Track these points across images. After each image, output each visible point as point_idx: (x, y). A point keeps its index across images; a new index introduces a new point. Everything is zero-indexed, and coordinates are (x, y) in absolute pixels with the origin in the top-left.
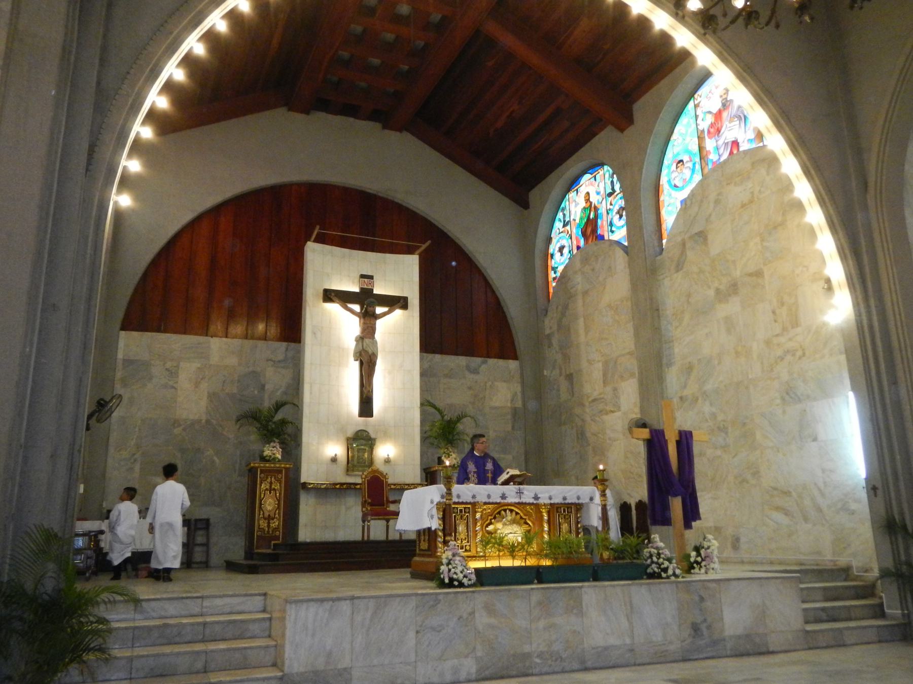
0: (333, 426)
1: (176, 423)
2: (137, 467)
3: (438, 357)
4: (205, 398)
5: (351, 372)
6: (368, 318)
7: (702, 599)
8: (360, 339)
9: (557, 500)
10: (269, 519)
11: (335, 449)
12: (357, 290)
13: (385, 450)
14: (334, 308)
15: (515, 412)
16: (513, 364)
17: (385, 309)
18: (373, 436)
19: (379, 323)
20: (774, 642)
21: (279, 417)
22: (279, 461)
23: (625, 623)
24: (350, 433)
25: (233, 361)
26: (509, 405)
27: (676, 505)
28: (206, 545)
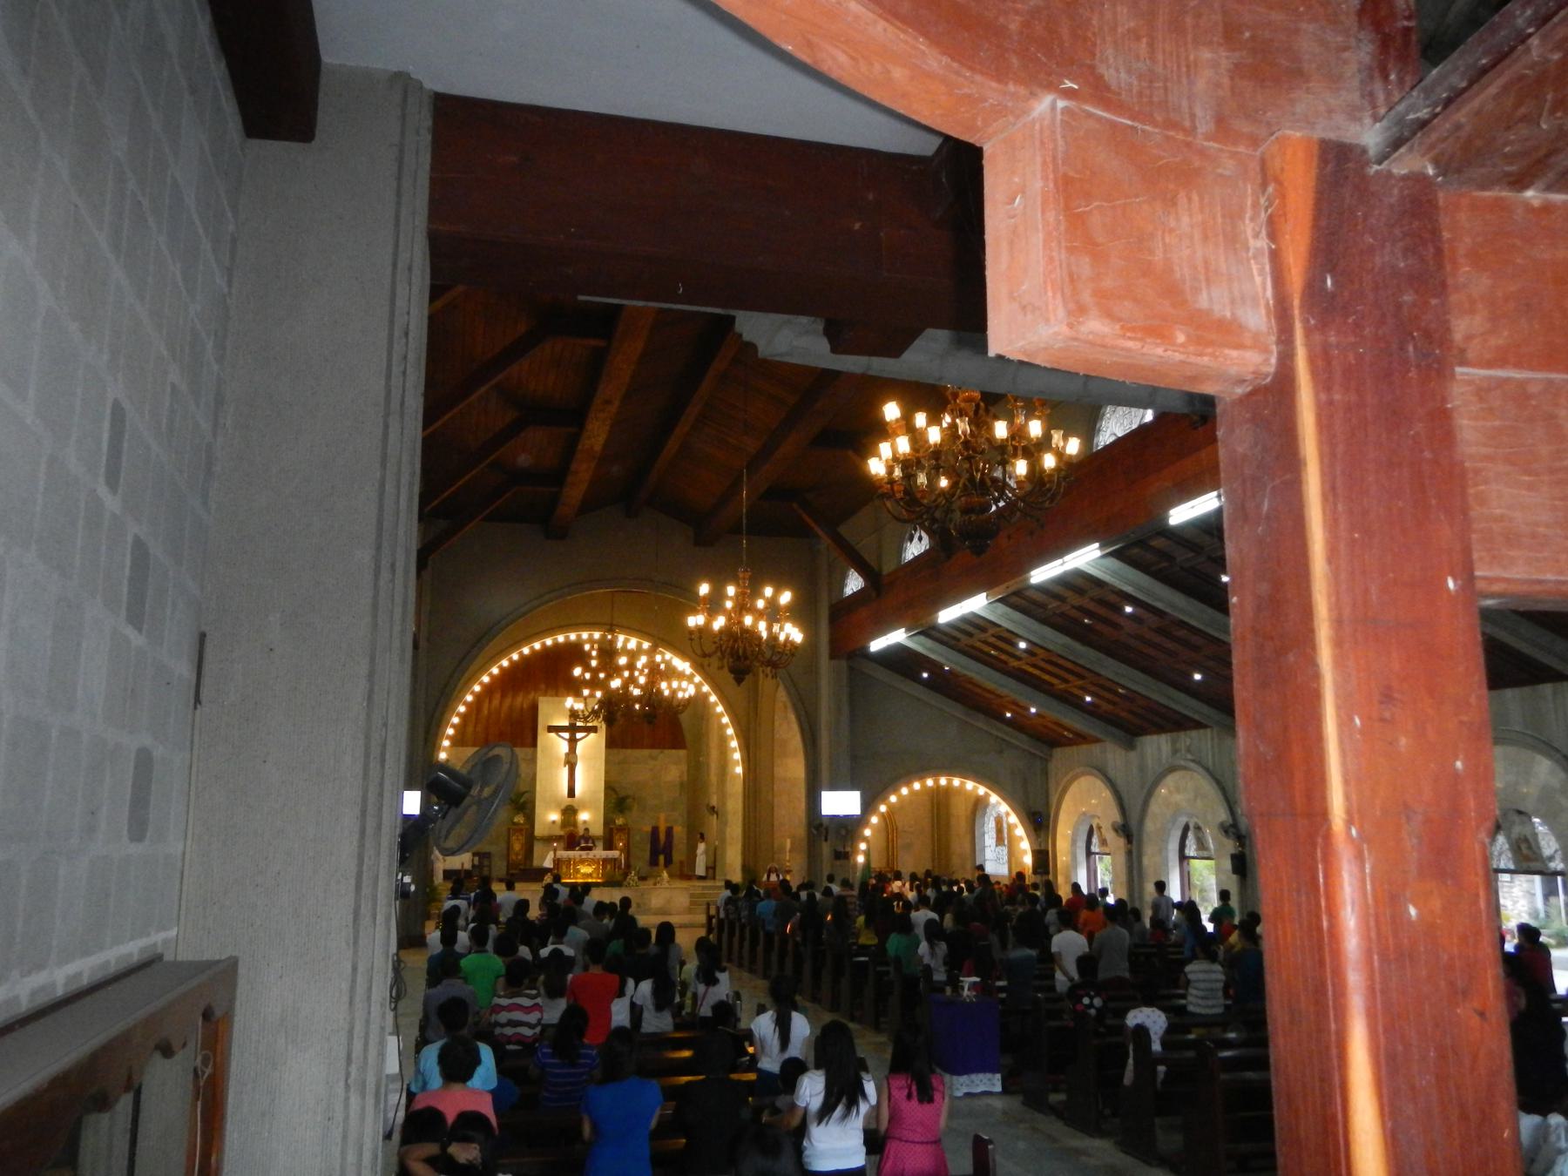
3: (629, 751)
5: (565, 771)
6: (573, 742)
8: (567, 755)
9: (604, 857)
10: (517, 854)
11: (554, 816)
12: (565, 723)
13: (584, 816)
14: (553, 735)
15: (682, 784)
16: (682, 753)
17: (583, 734)
18: (576, 807)
19: (578, 743)
22: (522, 824)
24: (563, 807)
26: (678, 779)
27: (662, 858)
28: (490, 866)
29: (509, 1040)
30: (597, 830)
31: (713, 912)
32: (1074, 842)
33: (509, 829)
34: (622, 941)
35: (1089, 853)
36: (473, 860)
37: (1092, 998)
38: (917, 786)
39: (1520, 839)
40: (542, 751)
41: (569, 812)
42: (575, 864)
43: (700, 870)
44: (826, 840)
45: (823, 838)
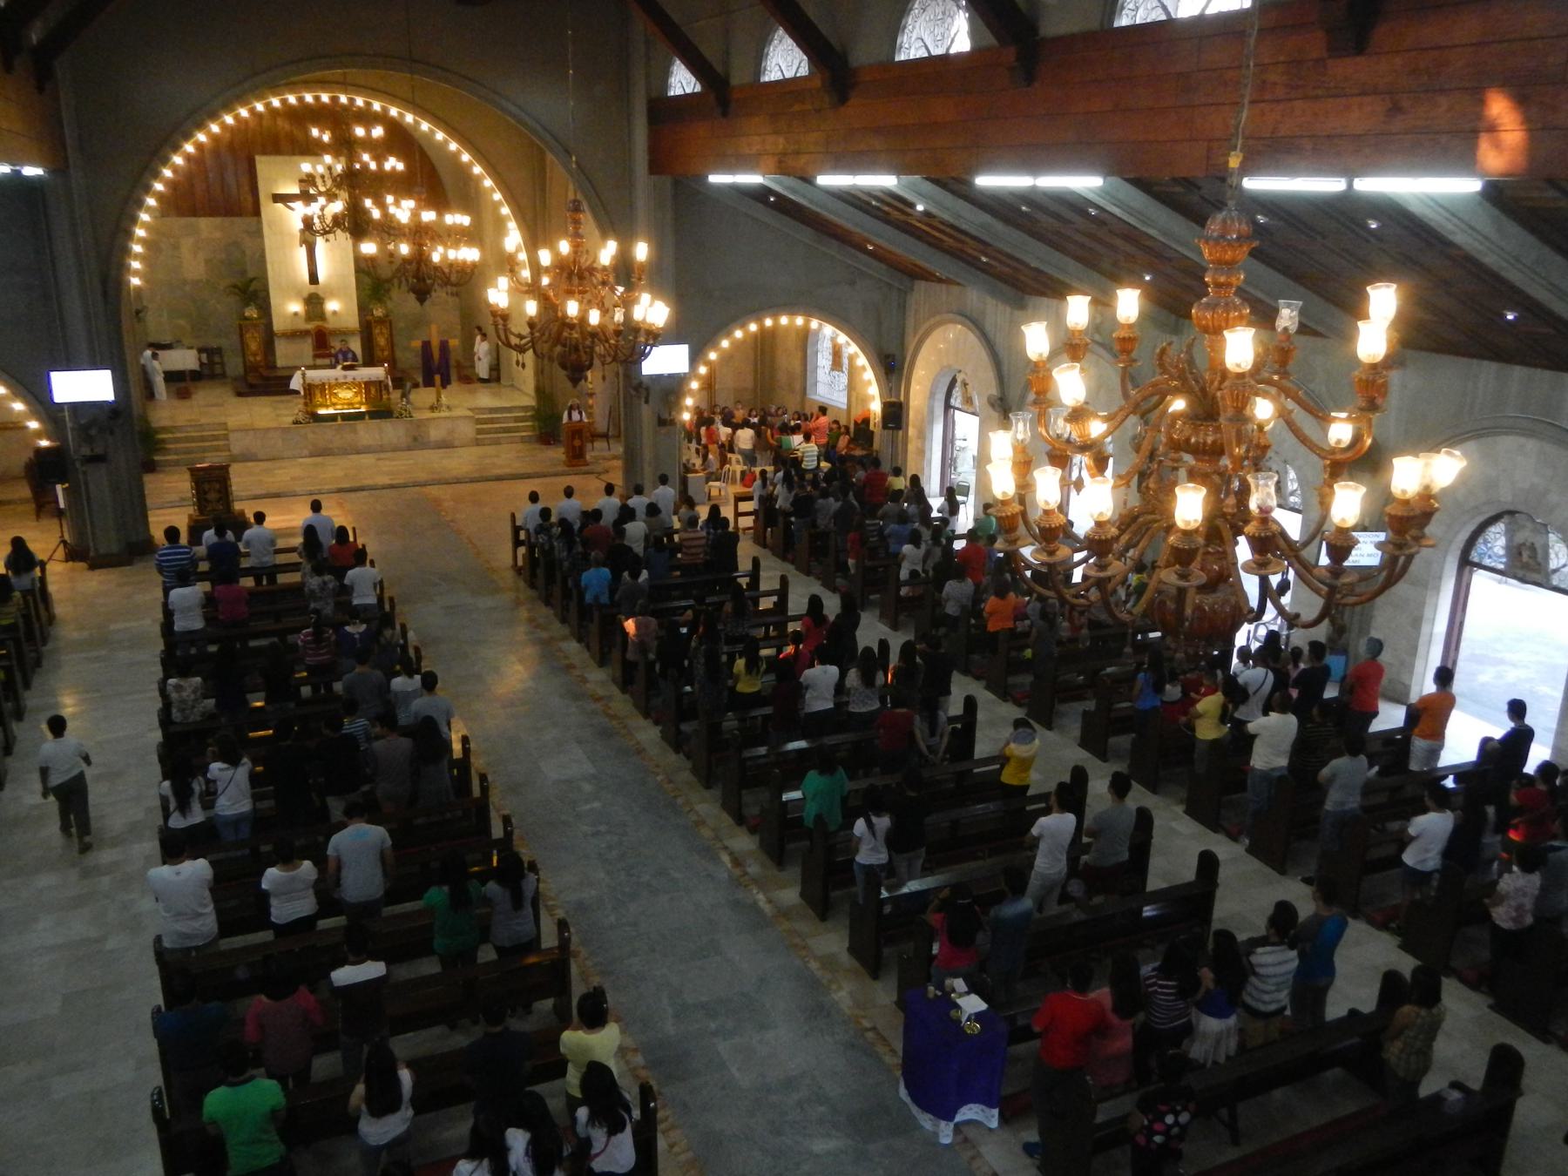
0: (292, 290)
1: (185, 282)
2: (165, 315)
4: (203, 264)
5: (302, 253)
7: (418, 426)
8: (302, 232)
10: (255, 355)
11: (296, 307)
13: (332, 306)
14: (280, 205)
18: (321, 295)
20: (457, 443)
21: (251, 289)
23: (377, 437)
24: (305, 294)
25: (218, 235)
27: (437, 378)
28: (222, 364)
30: (352, 321)
31: (518, 523)
32: (932, 395)
33: (241, 327)
34: (446, 889)
35: (948, 406)
36: (200, 359)
37: (1176, 1114)
38: (753, 327)
39: (1524, 544)
40: (269, 226)
41: (314, 303)
42: (331, 387)
43: (482, 369)
44: (647, 402)
45: (643, 400)
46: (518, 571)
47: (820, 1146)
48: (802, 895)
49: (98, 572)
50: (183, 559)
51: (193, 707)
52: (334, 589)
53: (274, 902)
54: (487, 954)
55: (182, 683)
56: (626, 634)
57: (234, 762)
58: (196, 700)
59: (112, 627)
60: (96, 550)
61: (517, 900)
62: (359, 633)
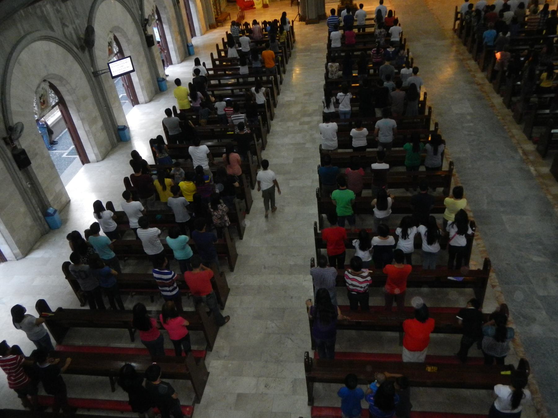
29: (353, 290)
31: (459, 10)
34: (412, 144)
46: (455, 30)
47: (536, 259)
48: (551, 170)
49: (309, 25)
50: (337, 21)
51: (335, 73)
52: (384, 35)
53: (353, 140)
54: (422, 169)
55: (333, 65)
56: (495, 59)
57: (345, 92)
58: (336, 71)
59: (312, 45)
60: (308, 18)
61: (436, 152)
62: (391, 51)
